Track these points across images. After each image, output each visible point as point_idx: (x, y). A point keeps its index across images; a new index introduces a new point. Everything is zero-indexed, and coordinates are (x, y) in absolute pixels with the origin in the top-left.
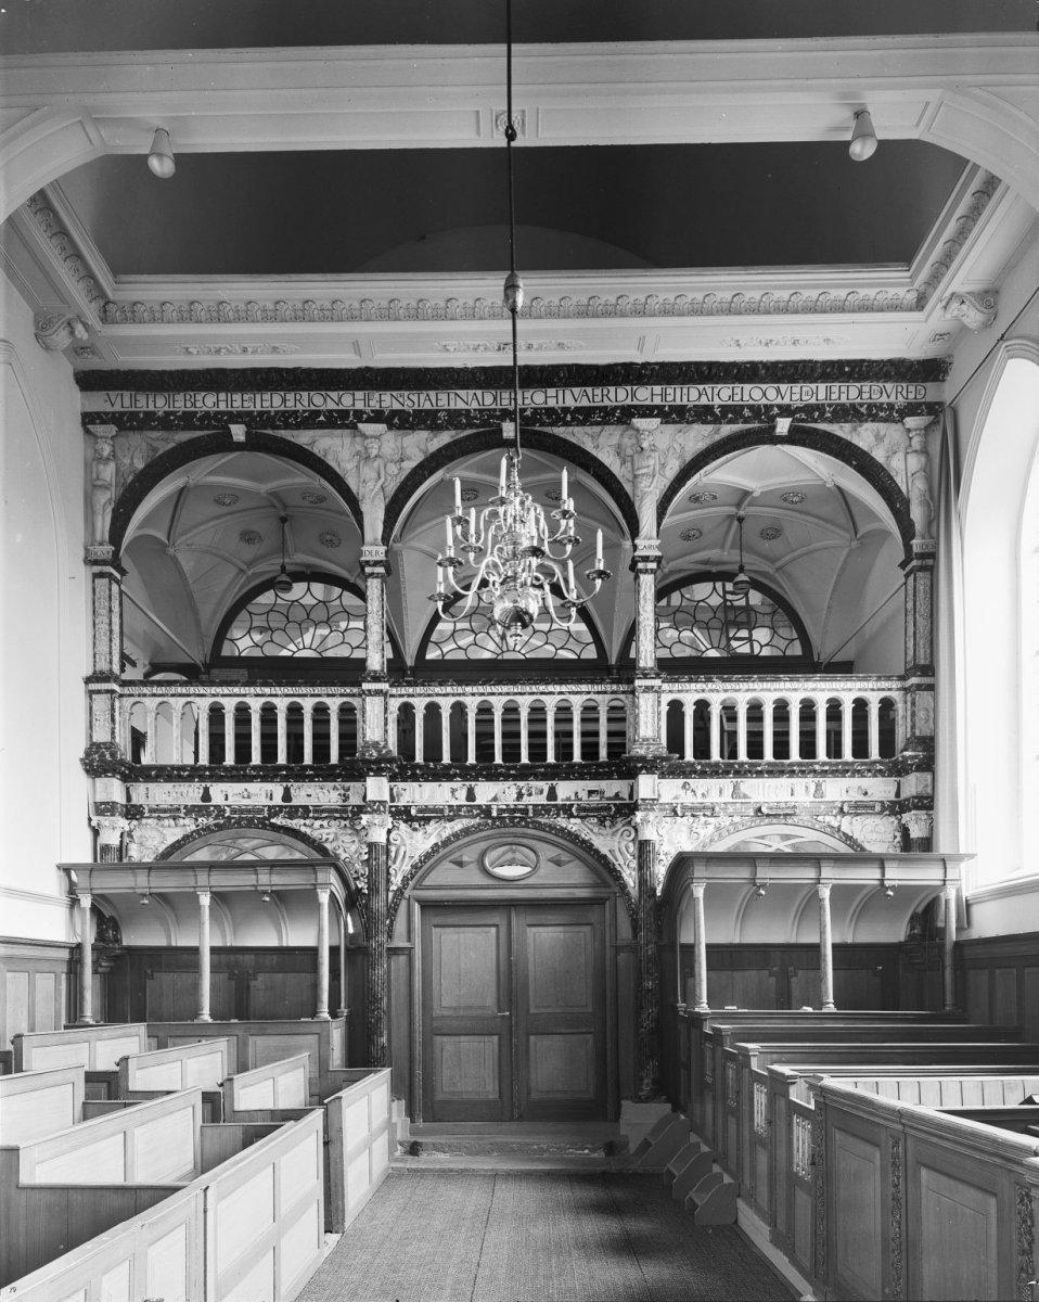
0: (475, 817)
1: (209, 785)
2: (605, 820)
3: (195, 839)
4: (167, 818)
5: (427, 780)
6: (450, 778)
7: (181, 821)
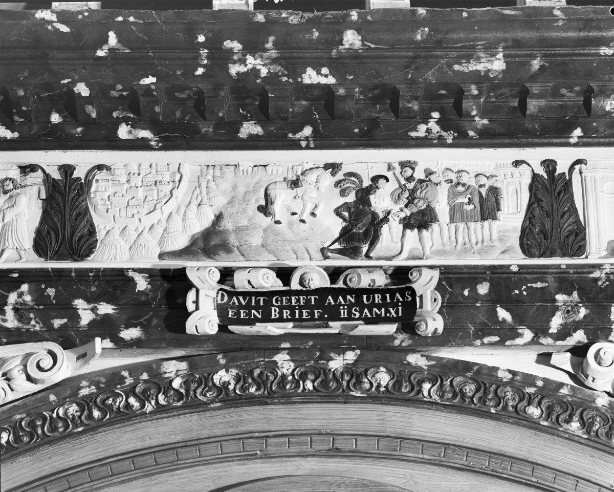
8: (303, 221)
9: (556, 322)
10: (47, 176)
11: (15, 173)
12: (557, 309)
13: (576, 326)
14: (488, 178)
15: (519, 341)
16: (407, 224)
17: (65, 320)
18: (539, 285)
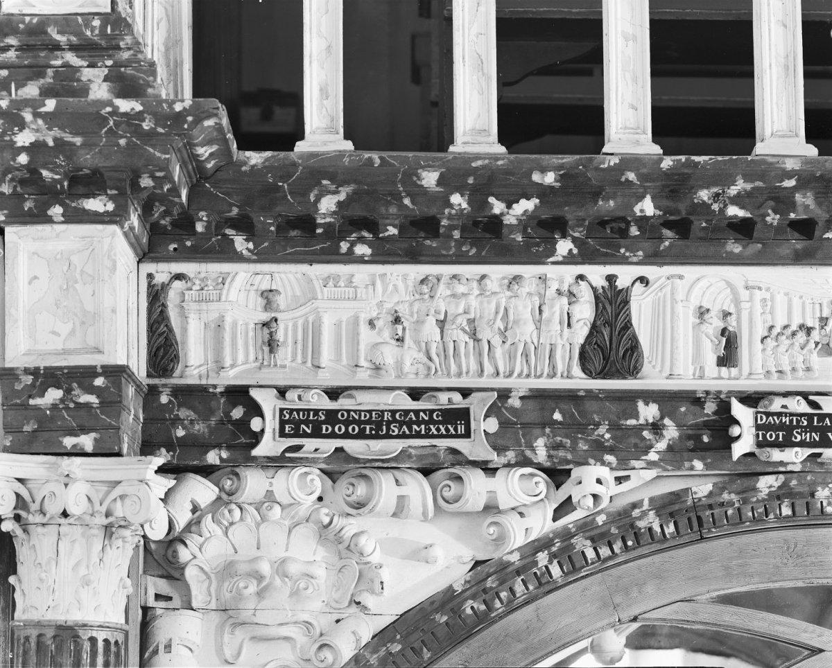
1: (625, 275)
3: (545, 585)
4: (385, 465)
7: (477, 487)
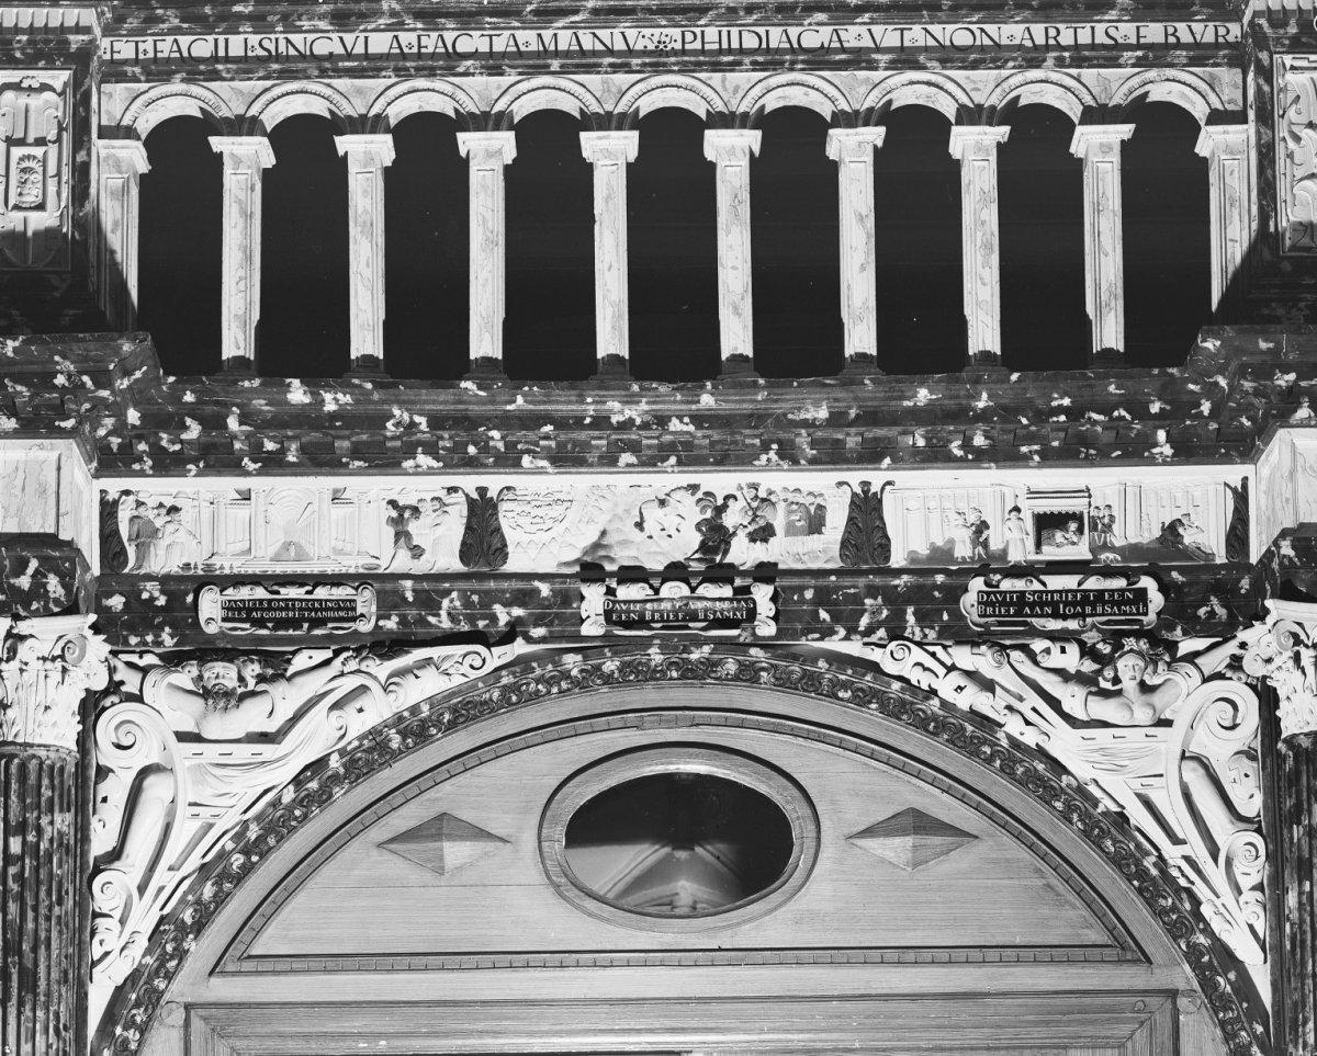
0: (507, 638)
2: (1118, 647)
5: (273, 464)
6: (384, 459)
8: (670, 536)
9: (864, 621)
10: (467, 495)
11: (442, 494)
12: (865, 610)
13: (879, 625)
14: (815, 496)
15: (835, 637)
16: (753, 538)
17: (487, 621)
18: (852, 591)
